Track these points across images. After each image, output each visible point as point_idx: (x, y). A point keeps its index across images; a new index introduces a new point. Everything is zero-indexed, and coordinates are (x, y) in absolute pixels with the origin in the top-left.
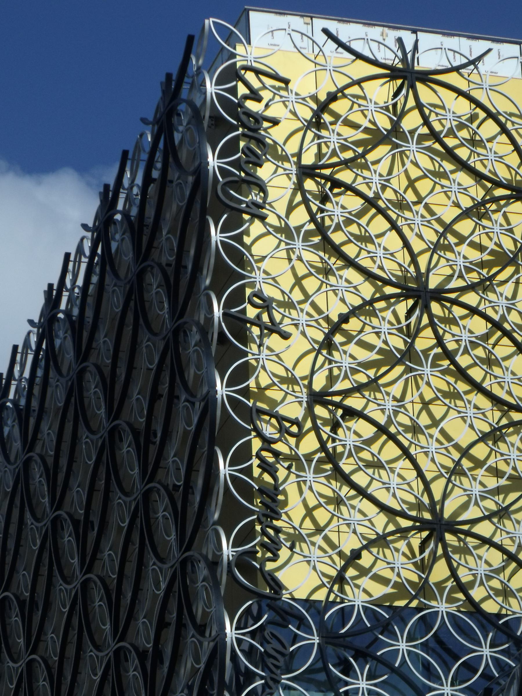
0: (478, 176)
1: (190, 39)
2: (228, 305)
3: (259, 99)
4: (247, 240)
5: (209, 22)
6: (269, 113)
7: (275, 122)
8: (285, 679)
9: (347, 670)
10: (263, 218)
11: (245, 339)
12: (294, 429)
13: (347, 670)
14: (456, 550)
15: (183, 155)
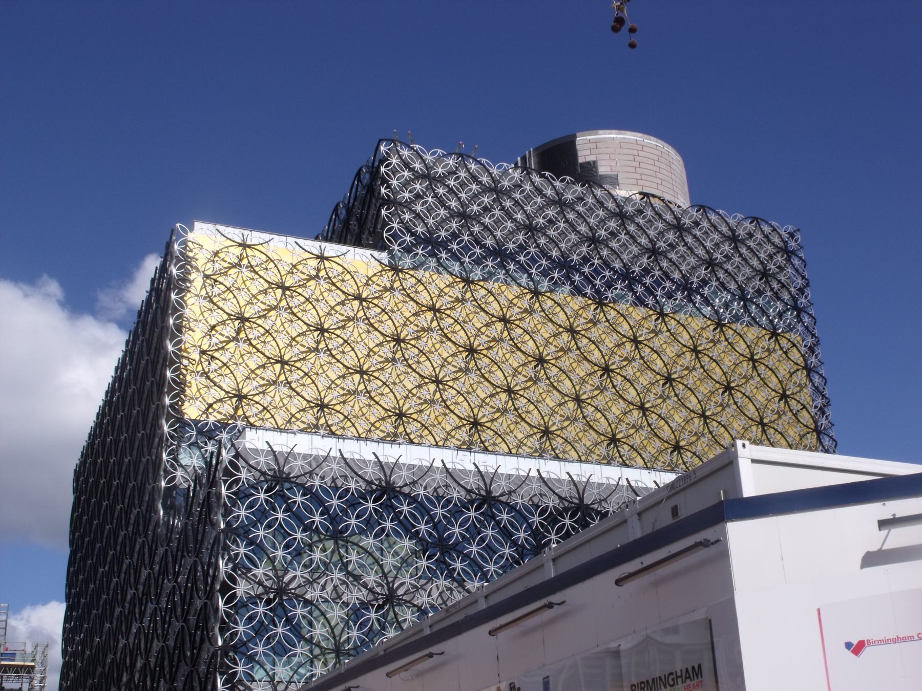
2: (176, 320)
4: (186, 299)
10: (190, 291)
11: (180, 331)
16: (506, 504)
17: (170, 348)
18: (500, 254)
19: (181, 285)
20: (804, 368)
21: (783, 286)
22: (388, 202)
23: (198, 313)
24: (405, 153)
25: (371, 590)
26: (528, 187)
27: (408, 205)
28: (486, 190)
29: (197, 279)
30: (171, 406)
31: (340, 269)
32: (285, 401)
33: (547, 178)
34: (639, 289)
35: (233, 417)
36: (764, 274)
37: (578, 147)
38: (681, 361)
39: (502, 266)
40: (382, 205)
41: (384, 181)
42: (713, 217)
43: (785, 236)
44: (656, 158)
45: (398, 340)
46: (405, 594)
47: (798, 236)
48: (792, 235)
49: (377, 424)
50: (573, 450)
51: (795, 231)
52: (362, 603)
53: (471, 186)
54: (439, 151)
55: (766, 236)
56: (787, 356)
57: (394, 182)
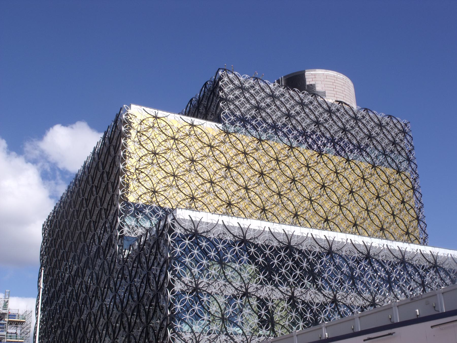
0: (166, 135)
1: (121, 108)
2: (124, 153)
3: (131, 119)
4: (127, 142)
5: (124, 106)
6: (133, 122)
7: (134, 123)
8: (128, 215)
9: (138, 214)
10: (130, 139)
11: (126, 158)
12: (133, 174)
13: (138, 214)
14: (157, 196)
15: (118, 127)
16: (253, 244)
17: (121, 167)
18: (243, 120)
19: (125, 135)
20: (412, 189)
21: (403, 149)
22: (222, 99)
23: (133, 150)
24: (231, 76)
25: (186, 285)
26: (257, 87)
27: (232, 101)
28: (238, 88)
29: (133, 133)
30: (123, 195)
31: (165, 124)
32: (136, 189)
33: (296, 91)
34: (338, 148)
35: (151, 202)
36: (394, 143)
37: (306, 77)
38: (357, 183)
39: (244, 126)
40: (220, 101)
41: (221, 89)
42: (371, 114)
43: (403, 124)
44: (336, 82)
45: (192, 161)
46: (203, 287)
47: (409, 125)
48: (406, 125)
49: (181, 202)
50: (276, 219)
51: (408, 123)
52: (182, 291)
53: (230, 86)
54: (247, 76)
55: (395, 124)
56: (404, 183)
57: (226, 90)
